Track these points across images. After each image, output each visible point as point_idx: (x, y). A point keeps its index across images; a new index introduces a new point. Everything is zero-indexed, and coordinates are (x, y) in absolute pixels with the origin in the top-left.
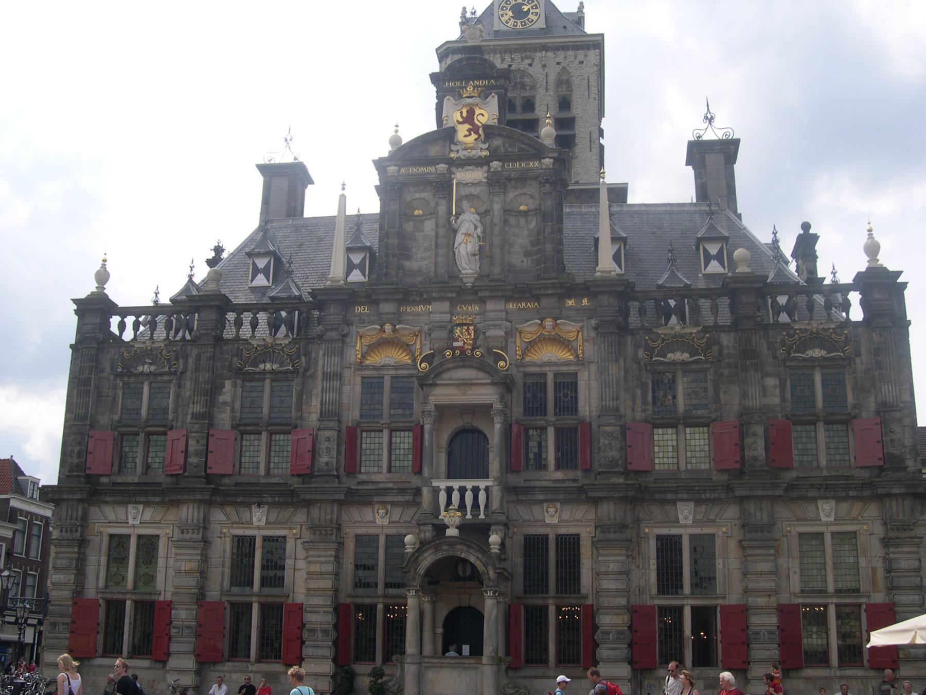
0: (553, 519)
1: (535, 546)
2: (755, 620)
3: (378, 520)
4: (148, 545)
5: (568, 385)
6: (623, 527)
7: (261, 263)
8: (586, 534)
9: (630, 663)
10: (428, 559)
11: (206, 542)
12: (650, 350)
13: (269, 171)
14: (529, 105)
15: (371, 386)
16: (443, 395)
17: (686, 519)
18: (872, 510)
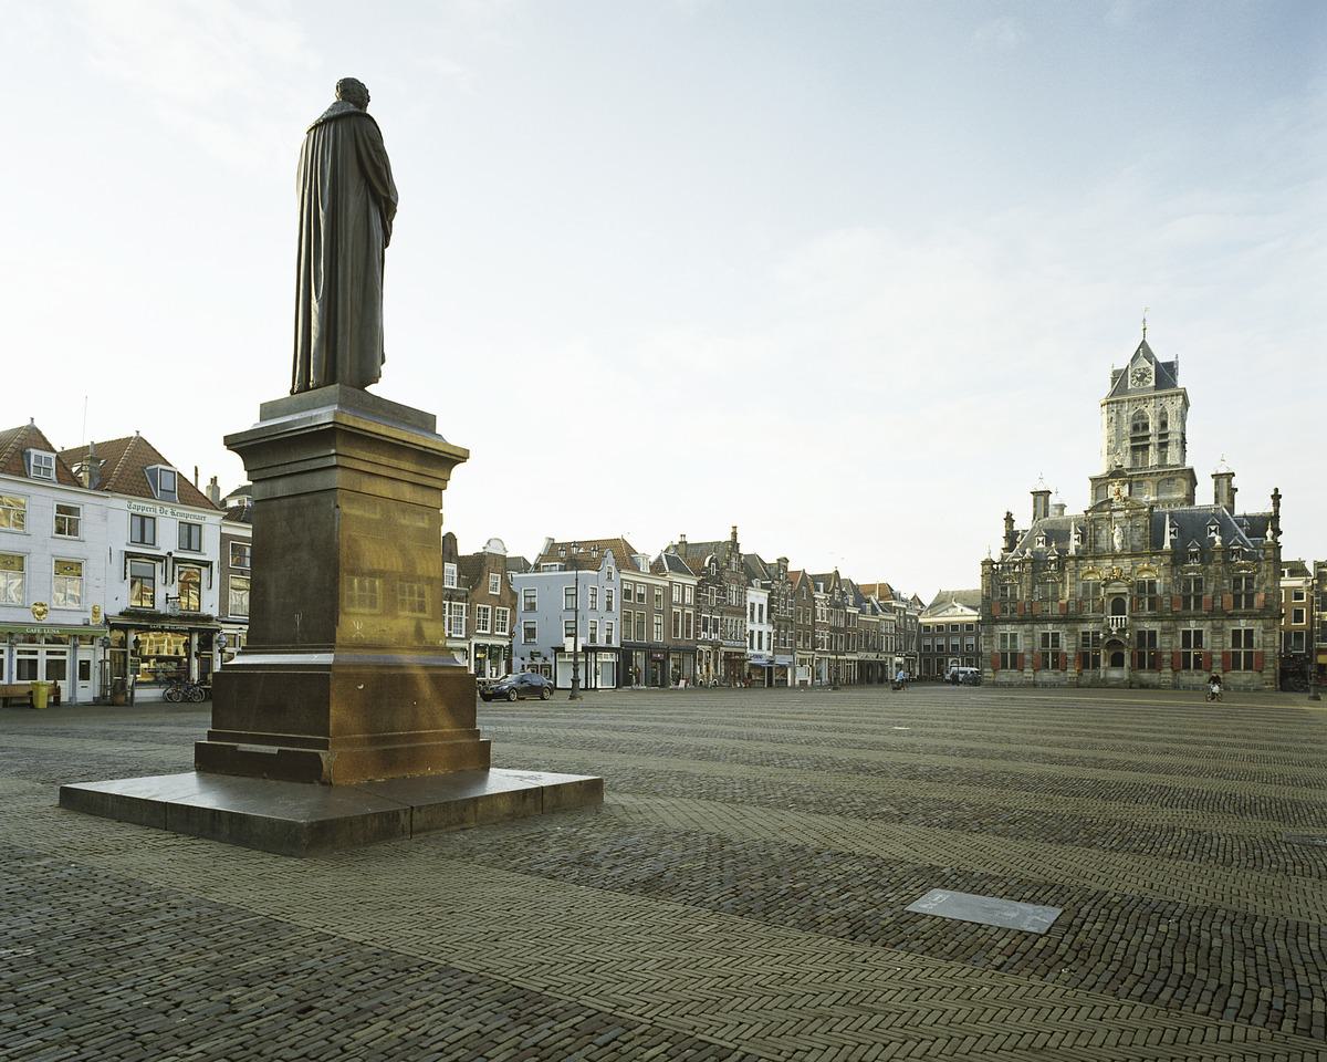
0: (1147, 626)
1: (1141, 634)
2: (1214, 656)
3: (1090, 627)
4: (1014, 637)
5: (1152, 583)
6: (1170, 628)
7: (1041, 539)
8: (1158, 631)
9: (1172, 668)
10: (1107, 640)
11: (1033, 635)
12: (1182, 572)
13: (1036, 494)
14: (1146, 427)
15: (1086, 587)
16: (1110, 590)
17: (1193, 626)
18: (1260, 622)
